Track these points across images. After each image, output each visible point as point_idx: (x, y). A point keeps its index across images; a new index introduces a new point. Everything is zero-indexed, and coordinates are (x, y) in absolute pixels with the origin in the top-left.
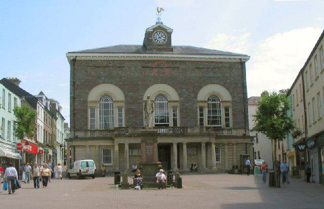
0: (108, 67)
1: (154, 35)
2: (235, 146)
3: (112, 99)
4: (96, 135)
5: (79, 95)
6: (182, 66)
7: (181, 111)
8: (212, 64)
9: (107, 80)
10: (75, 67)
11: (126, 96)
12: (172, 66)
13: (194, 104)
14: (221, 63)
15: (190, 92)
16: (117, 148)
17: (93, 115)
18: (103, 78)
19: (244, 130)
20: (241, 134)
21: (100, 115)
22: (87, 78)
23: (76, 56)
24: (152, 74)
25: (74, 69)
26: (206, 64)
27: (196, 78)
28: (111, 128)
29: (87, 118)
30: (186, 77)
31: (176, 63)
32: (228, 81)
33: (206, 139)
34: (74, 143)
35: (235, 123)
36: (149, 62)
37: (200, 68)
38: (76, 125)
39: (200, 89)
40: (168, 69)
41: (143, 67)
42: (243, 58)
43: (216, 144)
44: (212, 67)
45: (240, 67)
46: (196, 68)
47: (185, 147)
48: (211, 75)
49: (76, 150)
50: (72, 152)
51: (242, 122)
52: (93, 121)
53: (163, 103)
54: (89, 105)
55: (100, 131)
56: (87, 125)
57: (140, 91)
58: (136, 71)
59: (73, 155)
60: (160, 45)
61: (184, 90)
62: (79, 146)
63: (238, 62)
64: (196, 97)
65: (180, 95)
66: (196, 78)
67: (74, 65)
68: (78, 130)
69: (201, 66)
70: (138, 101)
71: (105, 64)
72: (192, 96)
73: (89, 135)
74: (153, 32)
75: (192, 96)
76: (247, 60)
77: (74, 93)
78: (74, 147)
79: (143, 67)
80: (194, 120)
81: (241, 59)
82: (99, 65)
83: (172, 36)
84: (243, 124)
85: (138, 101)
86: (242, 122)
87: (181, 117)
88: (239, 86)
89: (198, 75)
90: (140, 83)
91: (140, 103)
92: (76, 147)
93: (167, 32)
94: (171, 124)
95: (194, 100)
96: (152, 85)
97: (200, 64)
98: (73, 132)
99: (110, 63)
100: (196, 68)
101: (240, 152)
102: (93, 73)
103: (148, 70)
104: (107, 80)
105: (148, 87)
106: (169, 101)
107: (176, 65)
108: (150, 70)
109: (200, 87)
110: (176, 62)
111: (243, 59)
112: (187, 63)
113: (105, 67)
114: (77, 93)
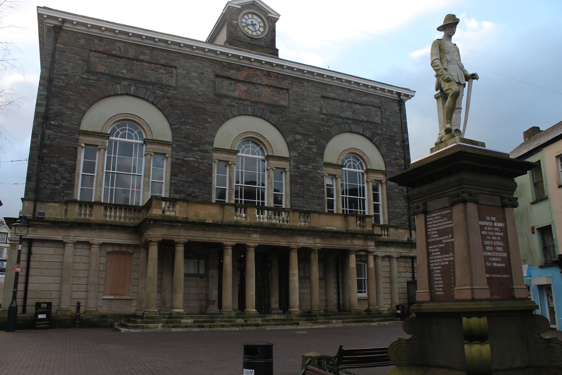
0: (138, 60)
1: (243, 17)
2: (395, 263)
3: (141, 136)
4: (98, 215)
5: (59, 114)
6: (295, 89)
7: (292, 181)
8: (351, 94)
9: (133, 88)
10: (58, 45)
11: (174, 131)
12: (274, 83)
13: (319, 169)
14: (367, 95)
15: (310, 143)
16: (154, 251)
17: (89, 167)
18: (125, 83)
19: (408, 231)
20: (405, 239)
21: (108, 168)
22: (84, 76)
23: (64, 21)
24: (236, 94)
25: (55, 49)
26: (341, 92)
27: (322, 116)
28: (133, 201)
29: (73, 170)
30: (302, 111)
31: (284, 79)
32: (379, 131)
33: (358, 243)
34: (32, 234)
35: (391, 215)
36: (230, 66)
37: (328, 98)
38: (42, 185)
39: (330, 140)
40: (267, 89)
41: (217, 76)
42: (403, 92)
43: (376, 257)
44: (350, 100)
45: (397, 108)
46: (322, 97)
47: (315, 258)
48: (349, 114)
49: (34, 250)
50: (24, 257)
51: (403, 215)
52: (88, 180)
53: (255, 159)
54: (84, 140)
55: (107, 206)
56: (71, 185)
57: (207, 125)
58: (201, 81)
59: (23, 264)
60: (252, 39)
61: (298, 137)
62: (43, 241)
63: (394, 100)
64: (322, 155)
65: (290, 146)
66: (322, 116)
67: (56, 39)
68: (51, 198)
69: (332, 95)
70: (201, 147)
71: (132, 53)
72: (315, 150)
73: (74, 213)
74: (239, 11)
75: (315, 150)
76: (408, 97)
77: (47, 106)
78: (30, 242)
79: (217, 76)
80: (318, 202)
81: (399, 94)
82: (118, 53)
83: (278, 24)
84: (405, 218)
85: (201, 147)
86: (403, 215)
87: (293, 195)
88: (398, 143)
89: (324, 111)
90: (208, 108)
91: (206, 151)
92: (34, 244)
93: (268, 18)
94: (269, 201)
95: (318, 159)
96: (234, 116)
97: (329, 89)
98: (30, 205)
99: (145, 54)
100: (323, 97)
101: (403, 275)
102: (102, 69)
103: (226, 83)
104: (133, 88)
105: (225, 118)
106: (268, 157)
107: (285, 84)
108: (231, 84)
109: (329, 137)
110: (285, 77)
111: (405, 95)
112: (305, 84)
113: (132, 60)
114: (56, 108)
